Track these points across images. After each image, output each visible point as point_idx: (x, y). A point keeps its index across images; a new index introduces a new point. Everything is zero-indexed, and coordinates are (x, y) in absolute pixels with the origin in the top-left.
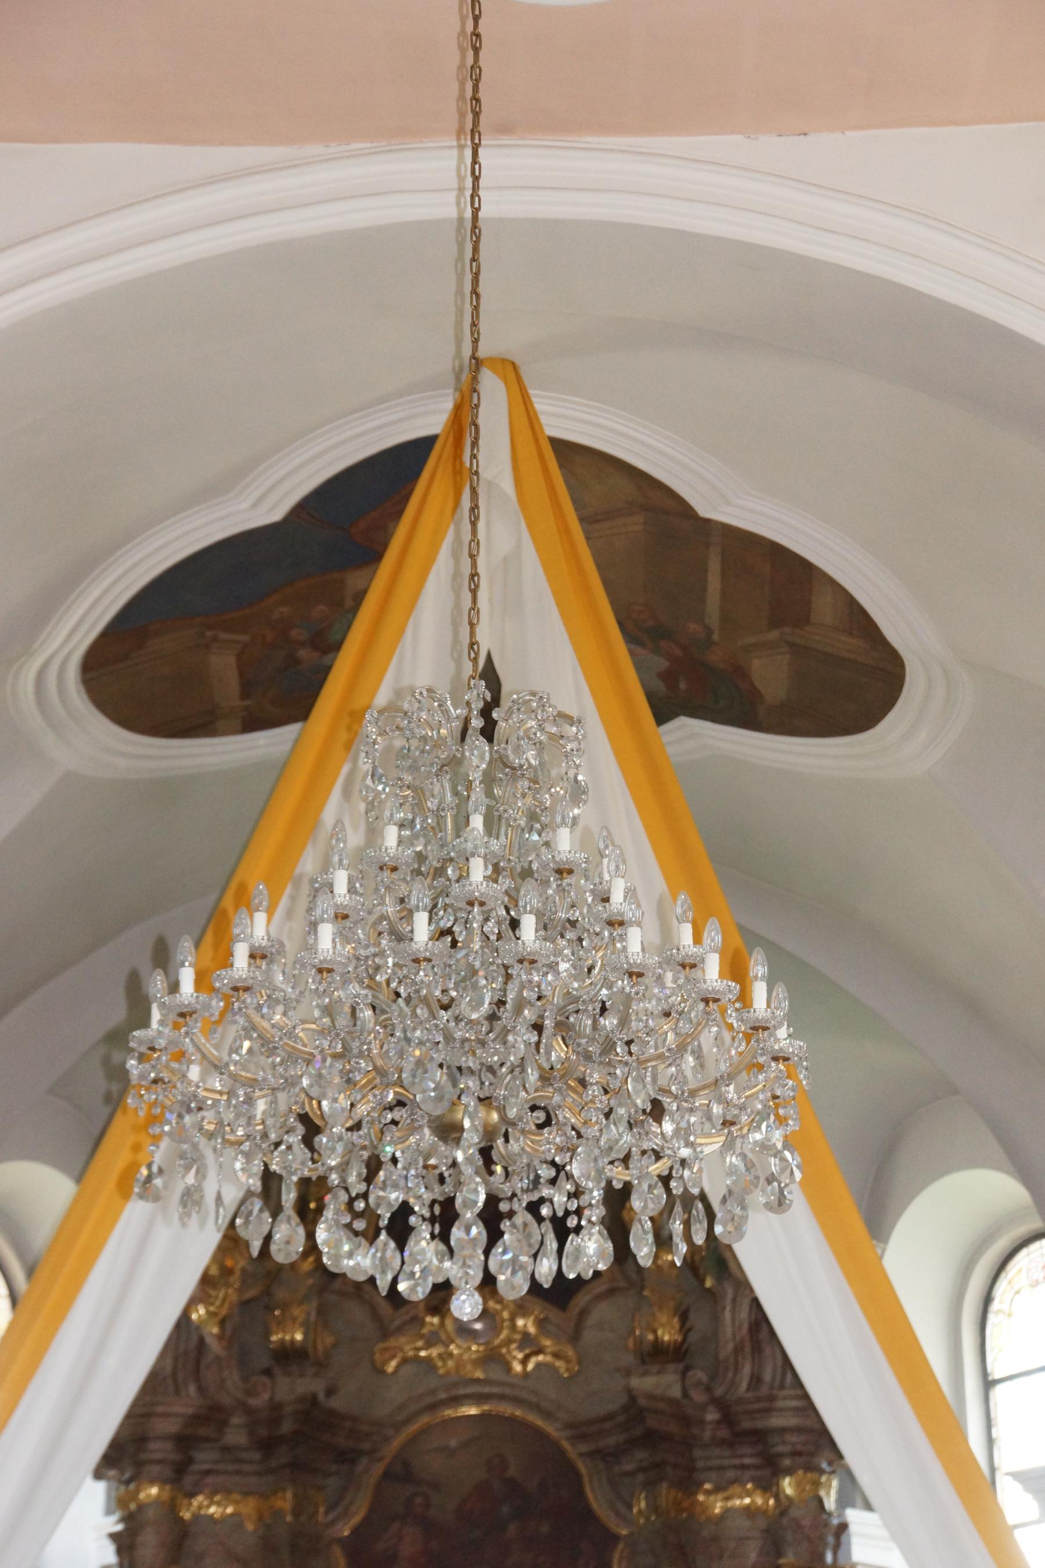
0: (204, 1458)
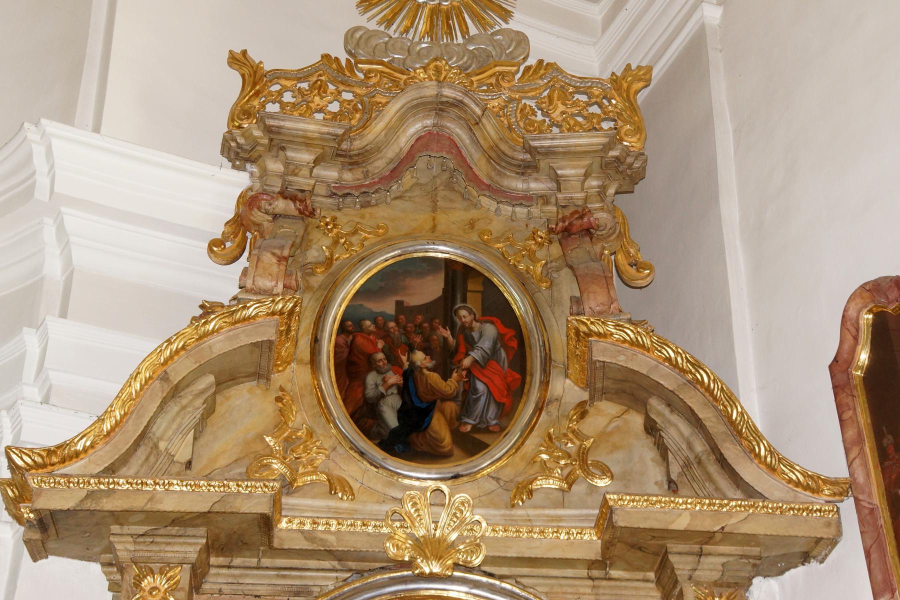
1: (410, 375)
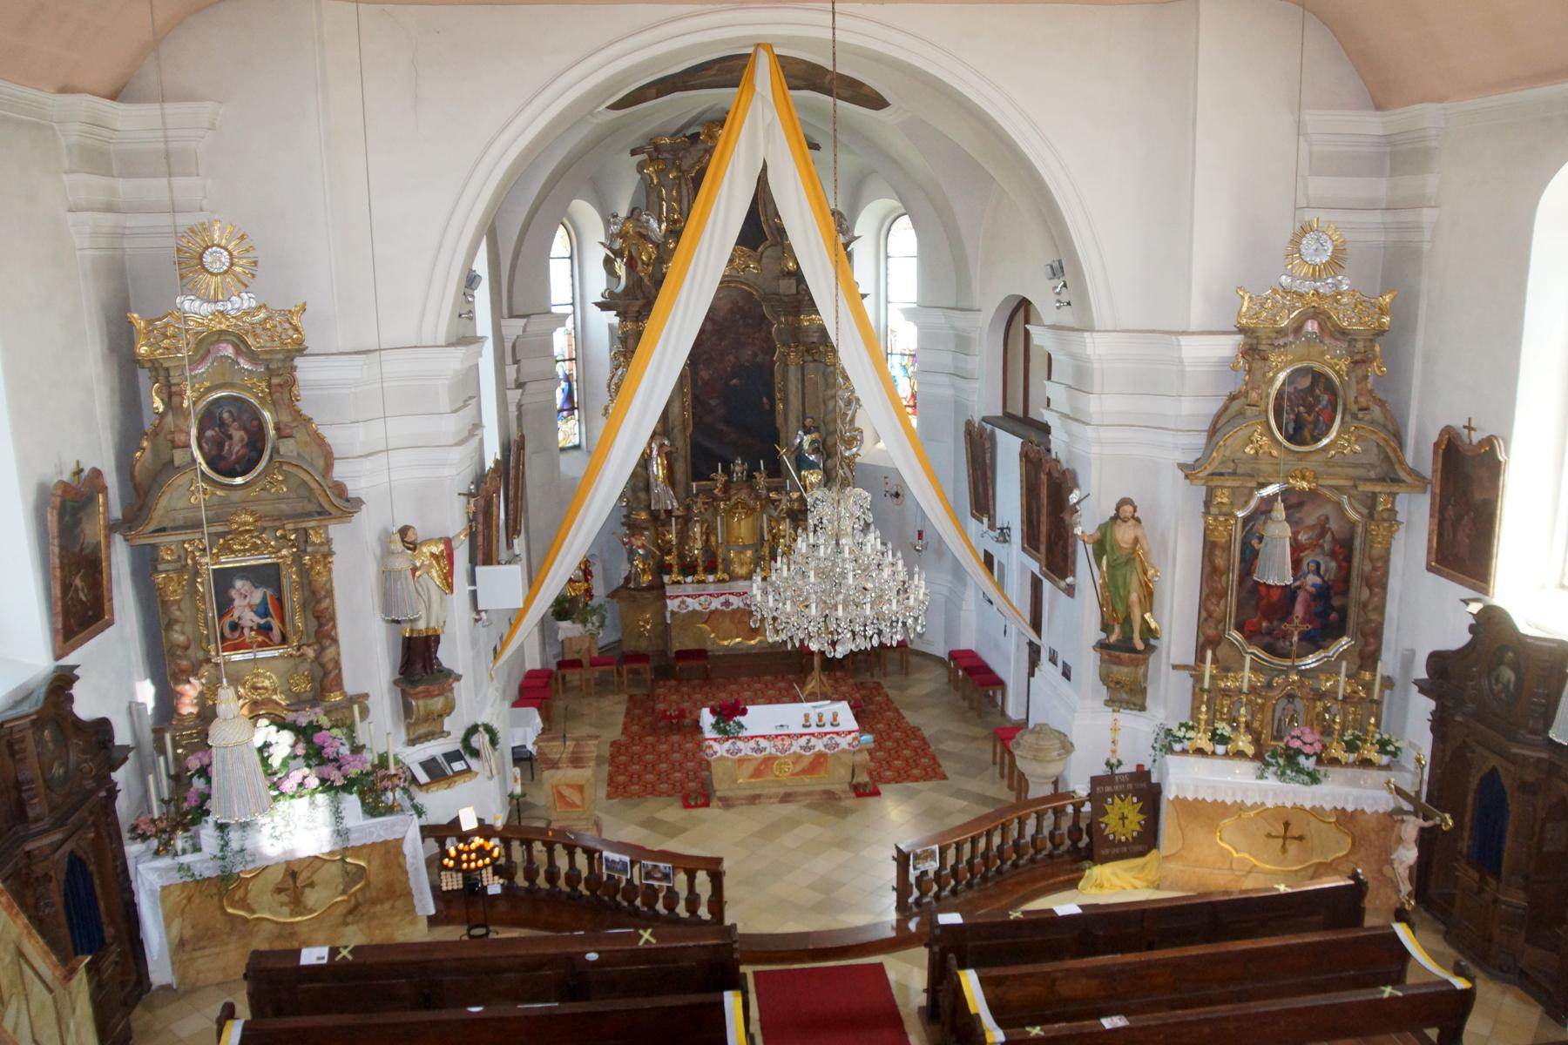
1: (1298, 415)
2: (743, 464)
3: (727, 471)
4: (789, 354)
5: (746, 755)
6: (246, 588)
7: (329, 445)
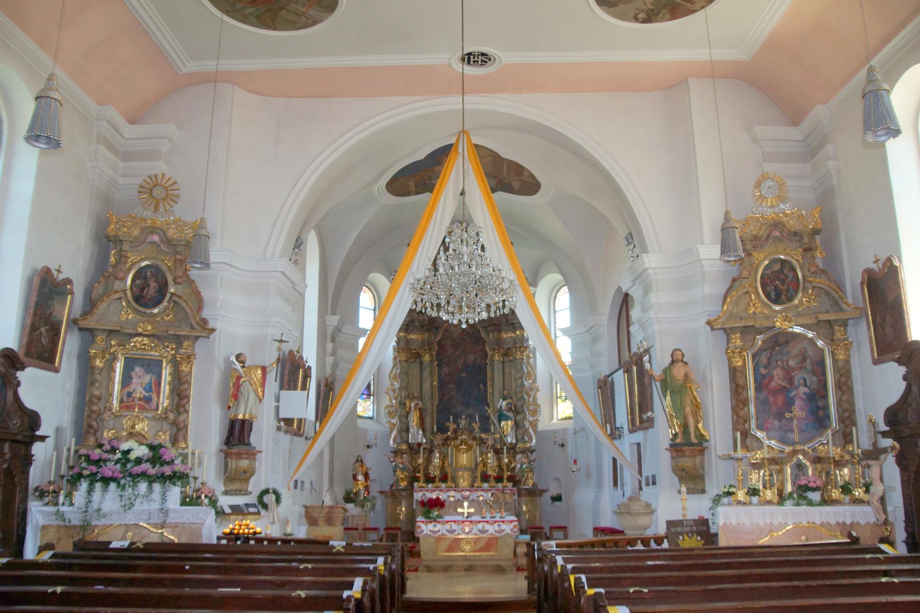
0: (411, 328)
1: (776, 287)
2: (466, 419)
3: (455, 422)
4: (494, 354)
5: (443, 534)
6: (141, 372)
7: (202, 297)
